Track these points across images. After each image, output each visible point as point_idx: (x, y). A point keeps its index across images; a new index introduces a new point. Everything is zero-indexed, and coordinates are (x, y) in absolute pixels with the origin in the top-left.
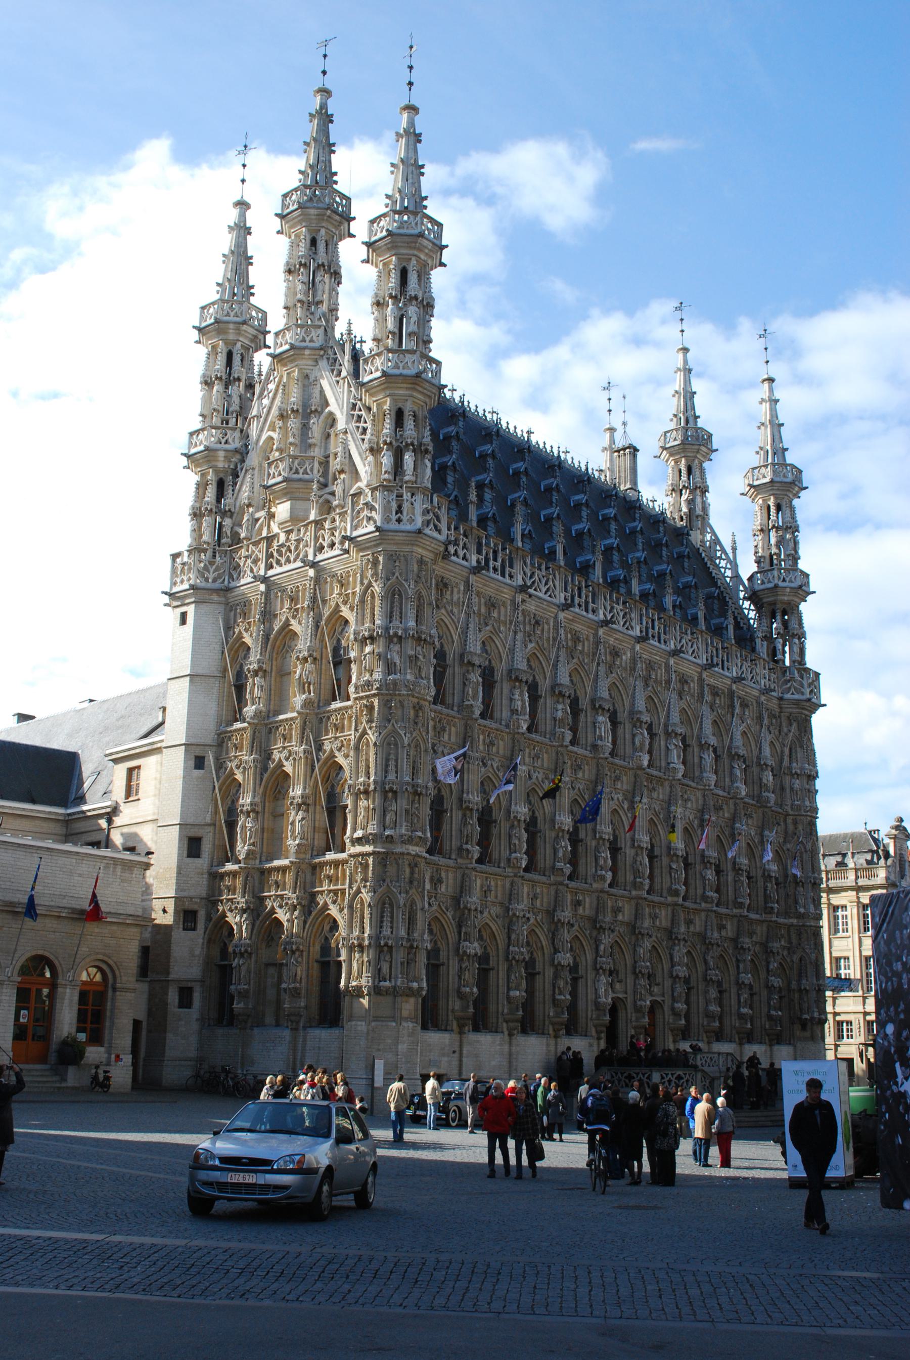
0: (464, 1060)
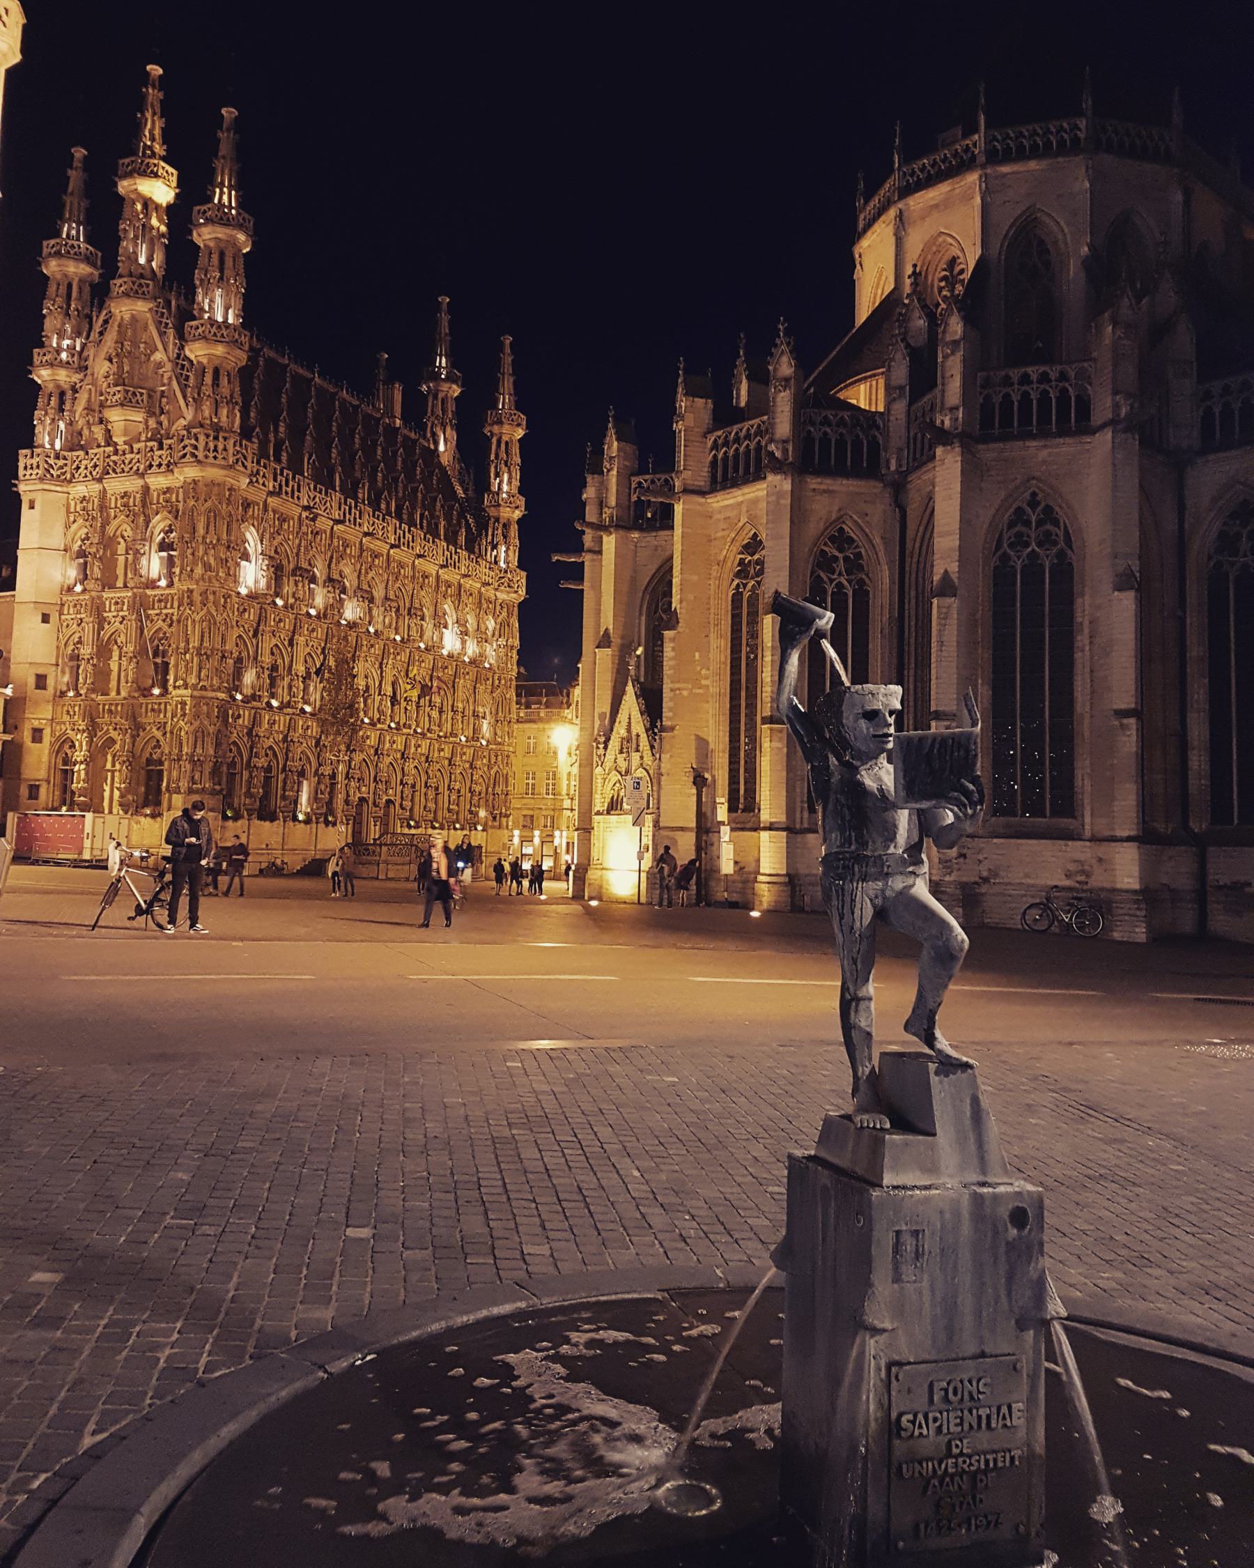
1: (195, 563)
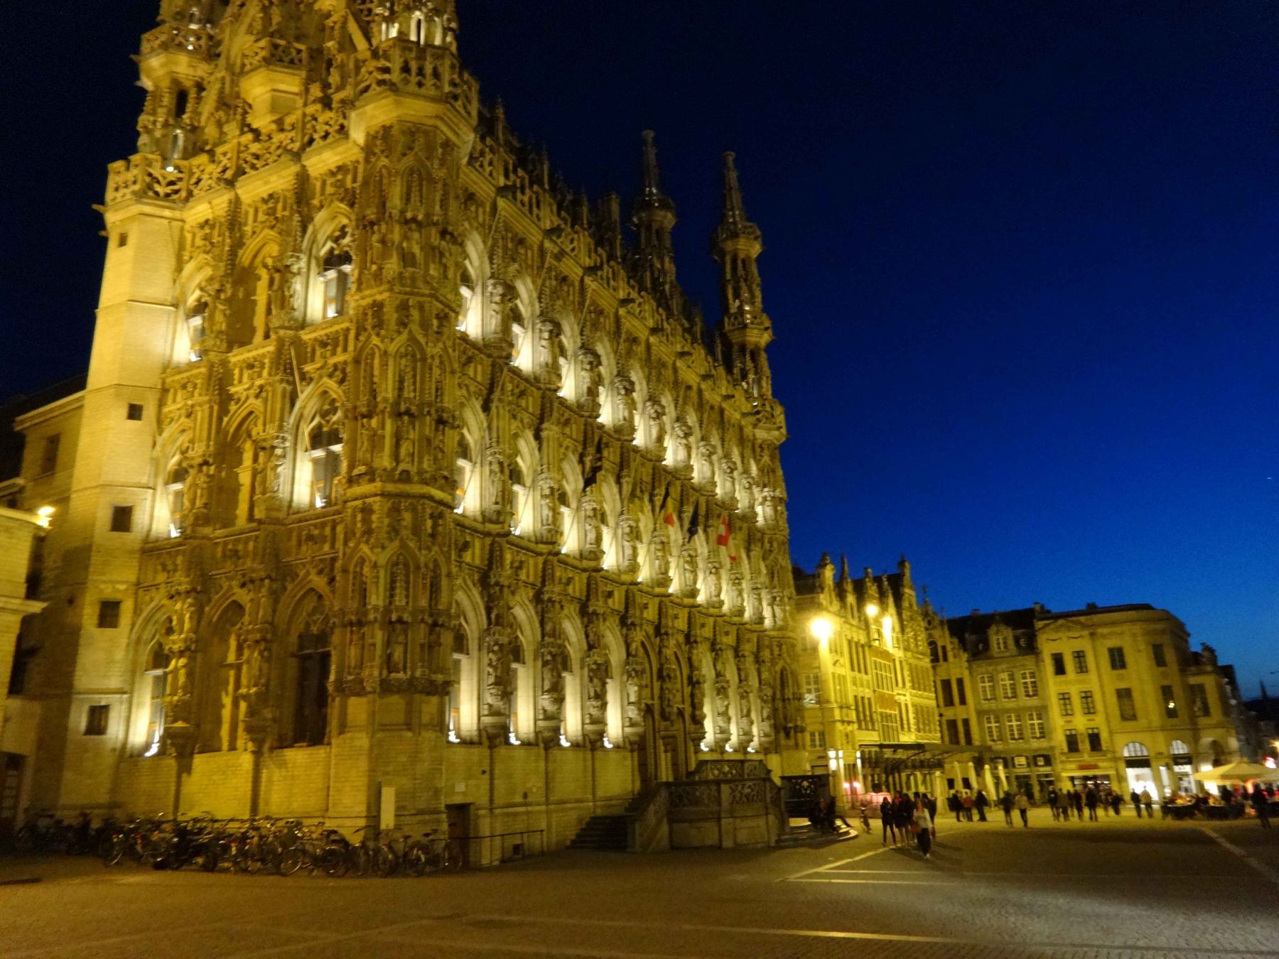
0: (496, 782)
1: (384, 255)
